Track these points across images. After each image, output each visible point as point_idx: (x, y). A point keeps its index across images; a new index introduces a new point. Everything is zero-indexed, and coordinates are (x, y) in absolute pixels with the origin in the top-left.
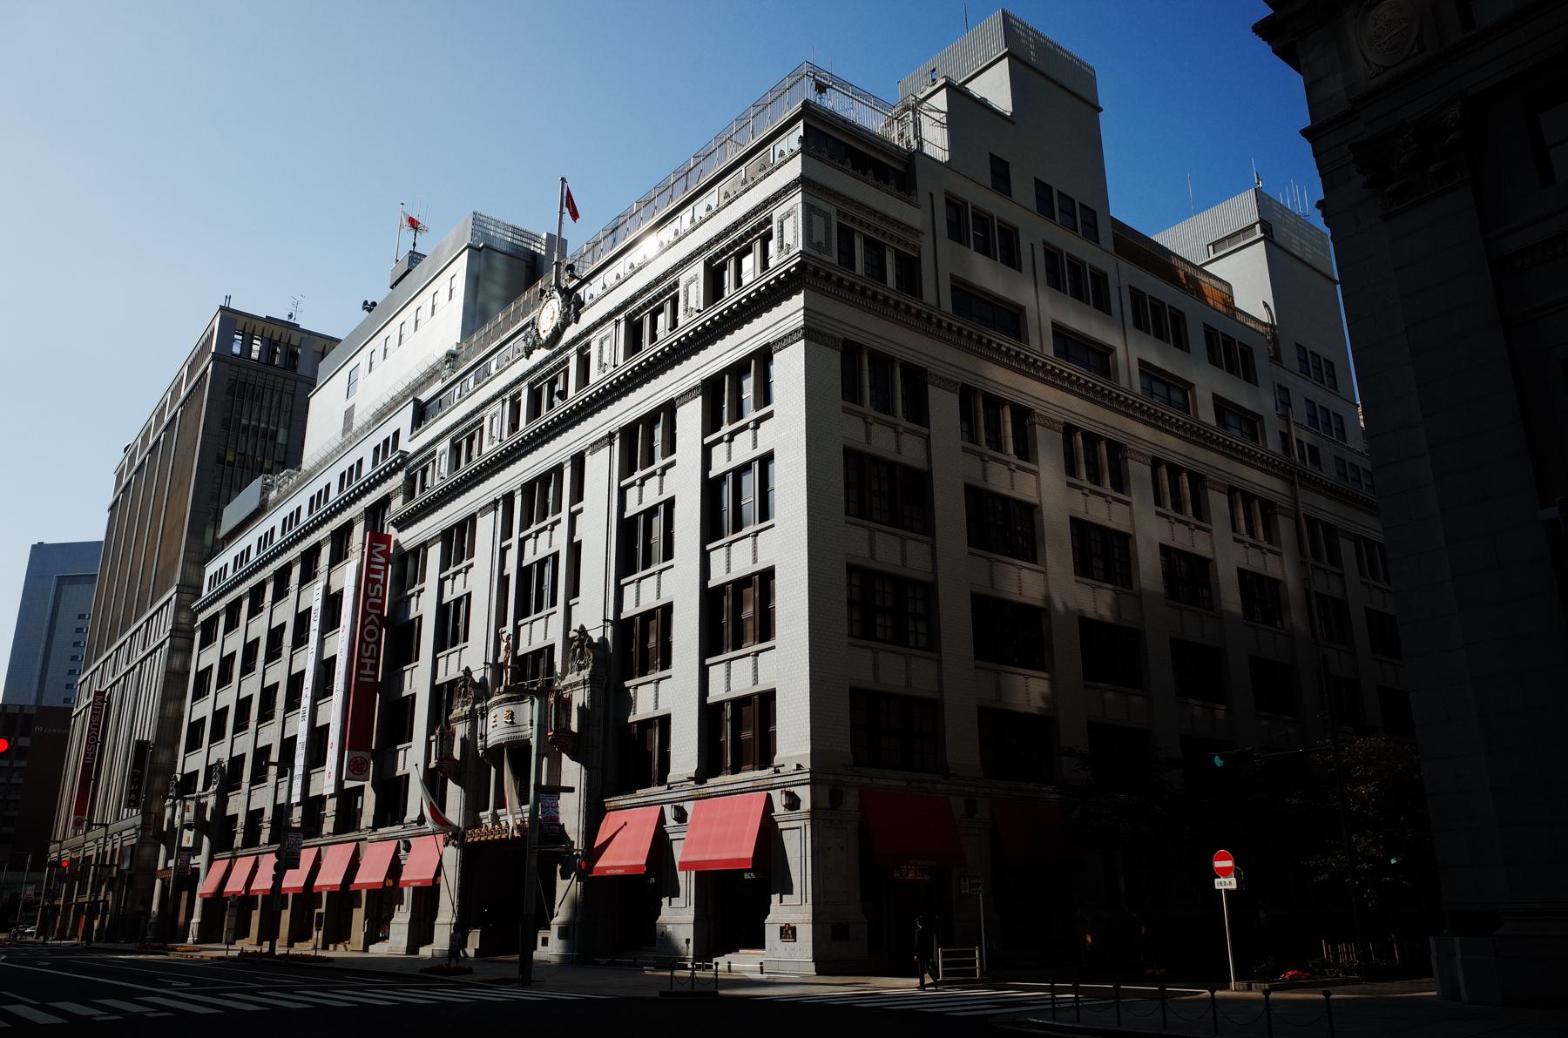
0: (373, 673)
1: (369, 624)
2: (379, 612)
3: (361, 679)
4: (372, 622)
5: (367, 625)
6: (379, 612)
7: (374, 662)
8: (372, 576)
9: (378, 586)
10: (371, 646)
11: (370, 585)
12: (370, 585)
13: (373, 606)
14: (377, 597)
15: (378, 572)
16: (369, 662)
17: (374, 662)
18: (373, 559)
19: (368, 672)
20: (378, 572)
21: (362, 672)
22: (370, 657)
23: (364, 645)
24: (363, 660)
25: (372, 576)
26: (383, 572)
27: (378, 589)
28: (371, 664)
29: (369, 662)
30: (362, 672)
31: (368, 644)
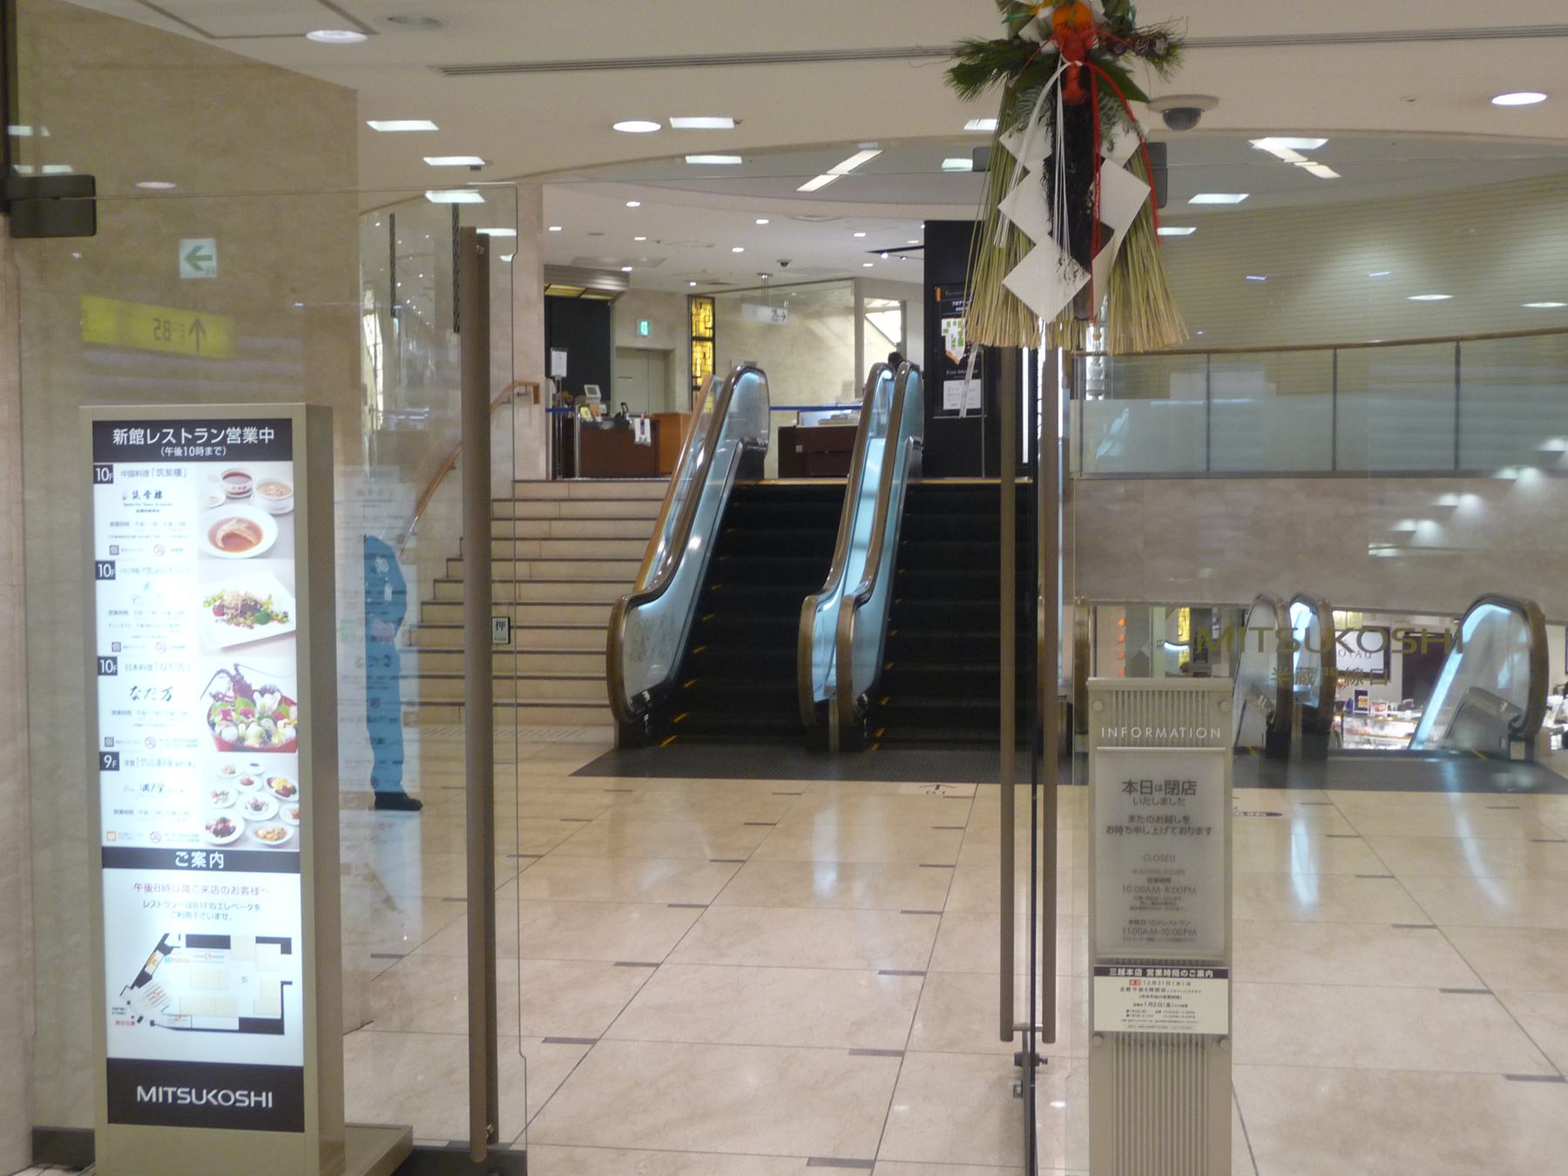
0: (264, 1094)
2: (205, 1092)
4: (215, 1097)
6: (205, 1092)
7: (252, 1094)
13: (199, 1097)
14: (190, 1093)
15: (165, 1094)
16: (253, 1099)
21: (264, 1105)
22: (248, 1096)
24: (253, 1104)
27: (182, 1092)
28: (255, 1096)
29: (253, 1099)
31: (236, 1101)
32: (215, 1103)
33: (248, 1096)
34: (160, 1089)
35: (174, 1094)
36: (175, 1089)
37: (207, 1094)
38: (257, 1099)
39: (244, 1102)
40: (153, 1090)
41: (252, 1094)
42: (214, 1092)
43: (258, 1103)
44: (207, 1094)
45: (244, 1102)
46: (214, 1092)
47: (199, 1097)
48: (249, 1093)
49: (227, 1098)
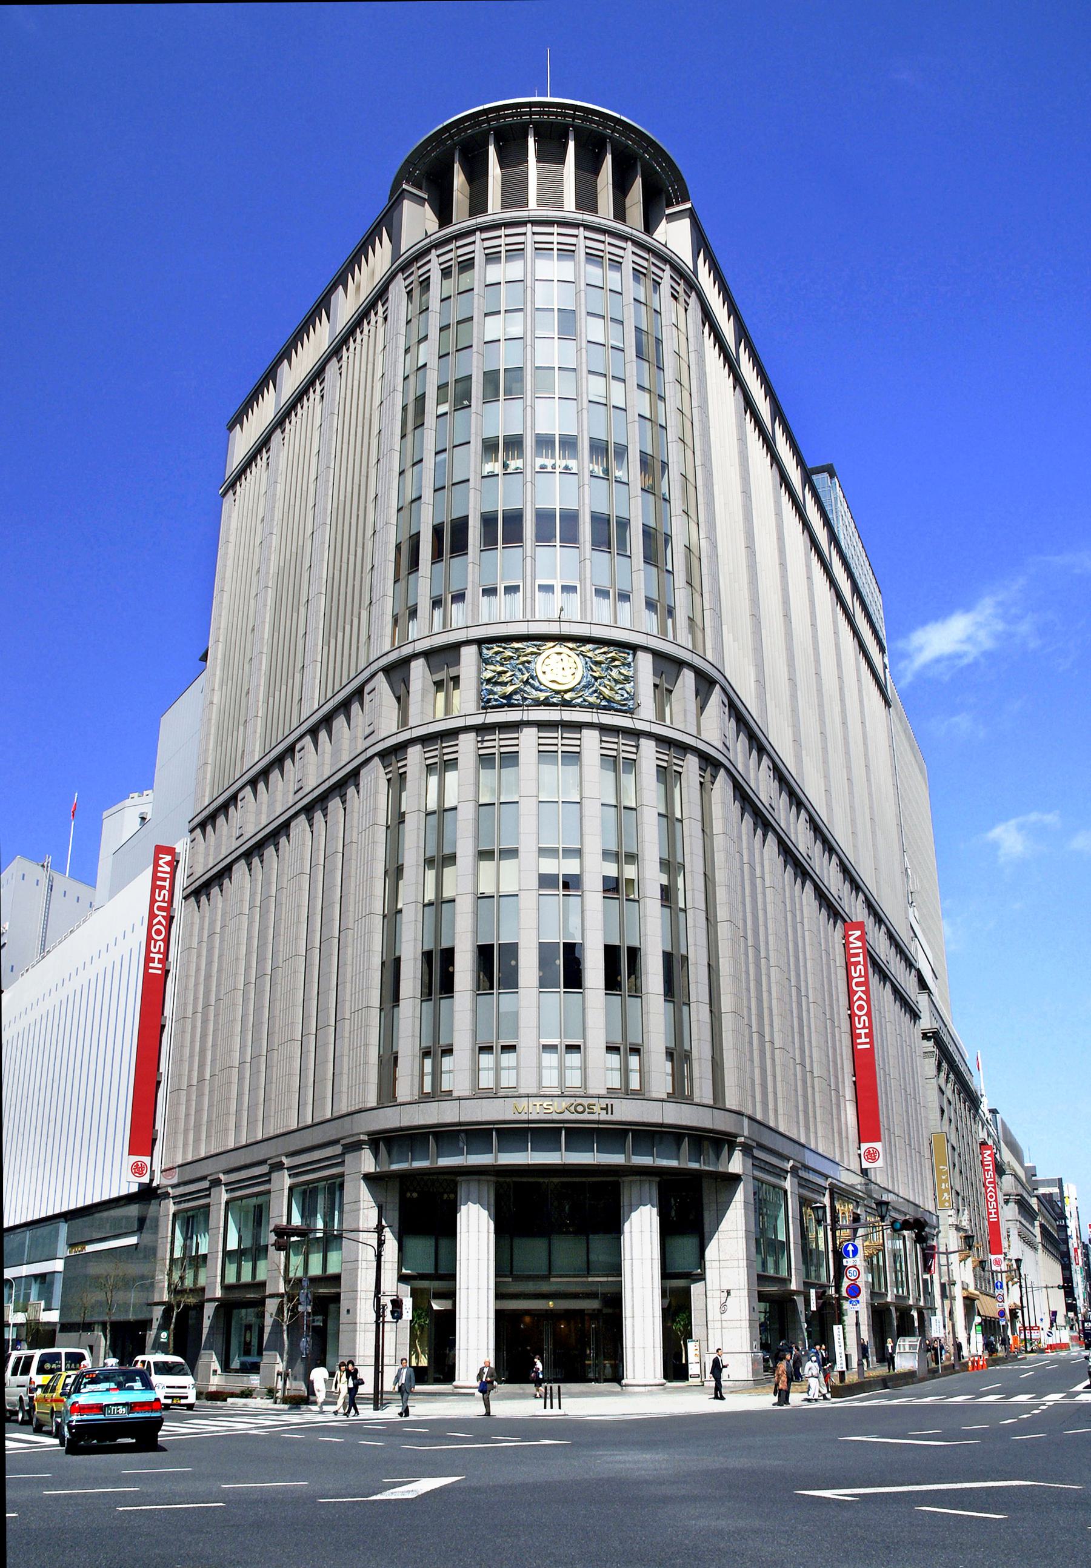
0: (160, 966)
1: (157, 924)
3: (151, 971)
4: (159, 923)
5: (156, 924)
7: (161, 956)
8: (159, 883)
9: (163, 892)
10: (159, 943)
11: (157, 891)
12: (157, 891)
13: (160, 908)
14: (163, 901)
15: (164, 879)
16: (157, 956)
17: (161, 956)
18: (160, 869)
19: (156, 965)
20: (164, 879)
21: (151, 965)
22: (159, 952)
23: (153, 942)
24: (152, 955)
25: (159, 883)
26: (168, 880)
29: (157, 956)
30: (151, 965)
31: (156, 941)
32: (155, 922)
33: (864, 1027)
34: (168, 876)
35: (164, 887)
36: (167, 888)
37: (162, 916)
38: (863, 1036)
39: (155, 947)
40: (168, 869)
41: (161, 956)
42: (164, 923)
43: (153, 960)
44: (162, 916)
45: (859, 1023)
46: (164, 923)
47: (160, 908)
48: (161, 953)
49: (158, 932)
